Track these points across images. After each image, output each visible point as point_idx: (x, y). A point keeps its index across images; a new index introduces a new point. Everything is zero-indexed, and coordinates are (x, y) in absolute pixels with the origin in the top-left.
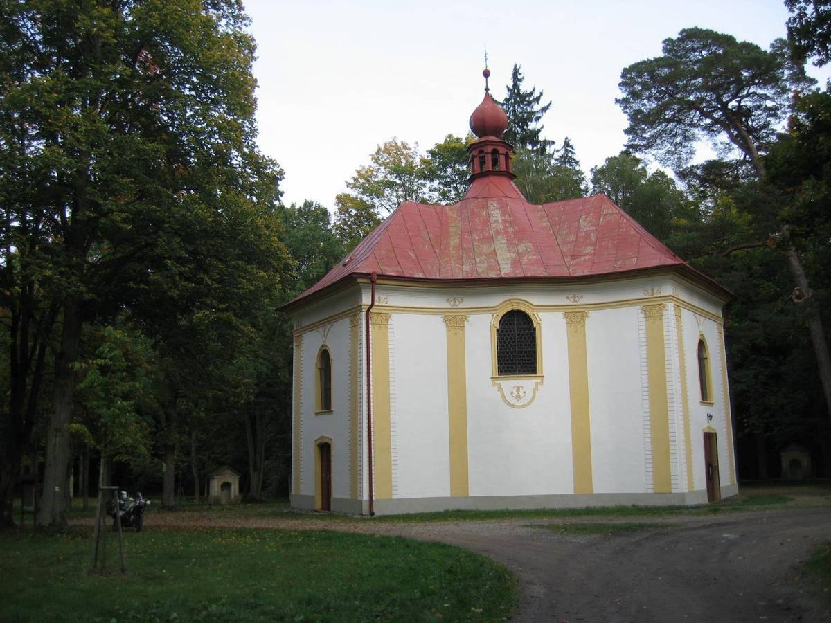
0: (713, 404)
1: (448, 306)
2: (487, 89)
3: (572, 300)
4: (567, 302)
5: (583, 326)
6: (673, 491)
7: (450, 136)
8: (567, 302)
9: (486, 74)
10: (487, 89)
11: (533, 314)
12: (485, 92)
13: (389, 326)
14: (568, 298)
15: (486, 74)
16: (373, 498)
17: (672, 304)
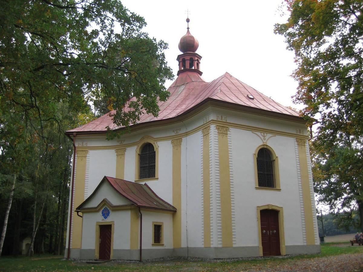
0: (280, 190)
1: (118, 144)
2: (188, 28)
3: (176, 132)
4: (173, 134)
5: (180, 147)
6: (212, 246)
7: (200, 57)
8: (173, 134)
9: (188, 21)
10: (188, 28)
11: (154, 143)
12: (187, 29)
13: (87, 158)
14: (173, 131)
15: (188, 21)
16: (71, 247)
17: (214, 126)
